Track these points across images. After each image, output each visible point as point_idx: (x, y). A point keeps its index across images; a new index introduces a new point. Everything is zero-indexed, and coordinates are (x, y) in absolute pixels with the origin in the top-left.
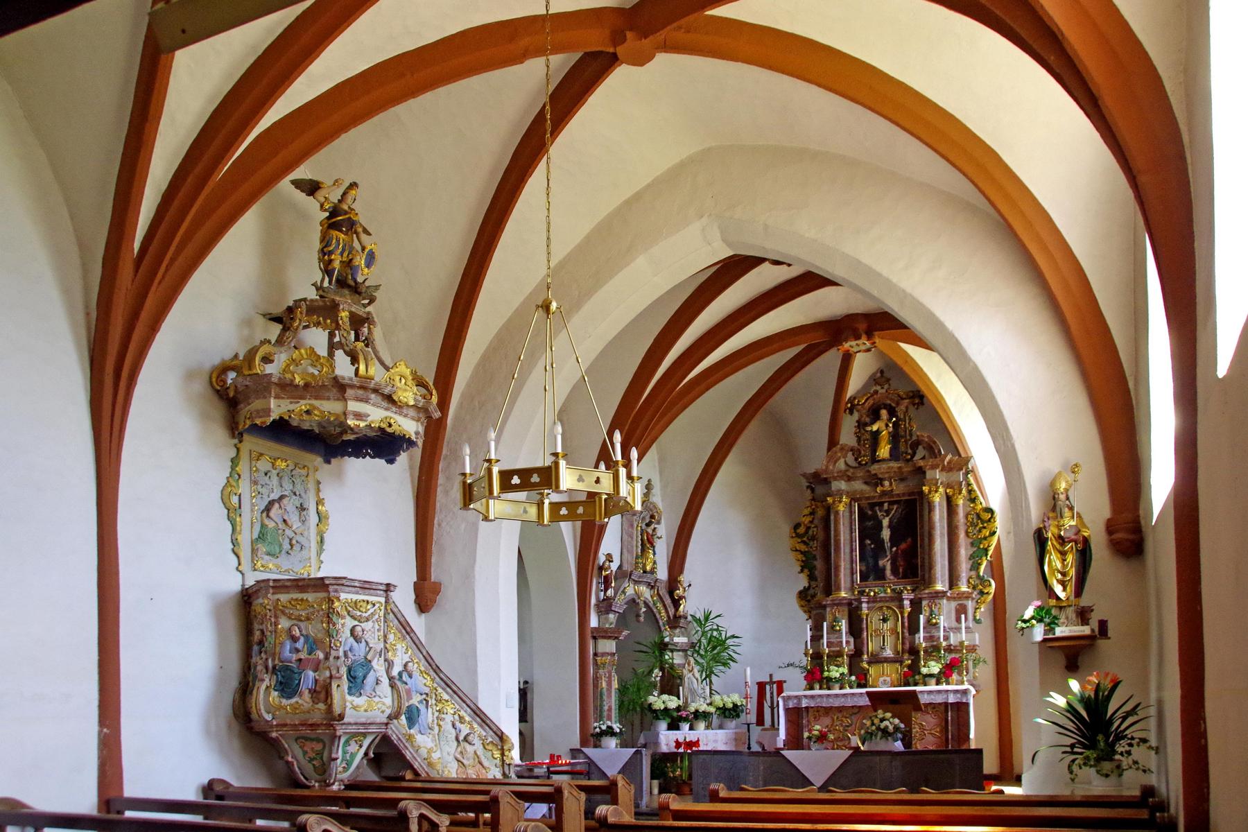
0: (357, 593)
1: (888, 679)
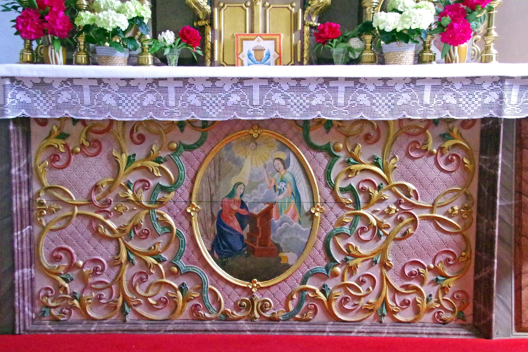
1: (269, 46)
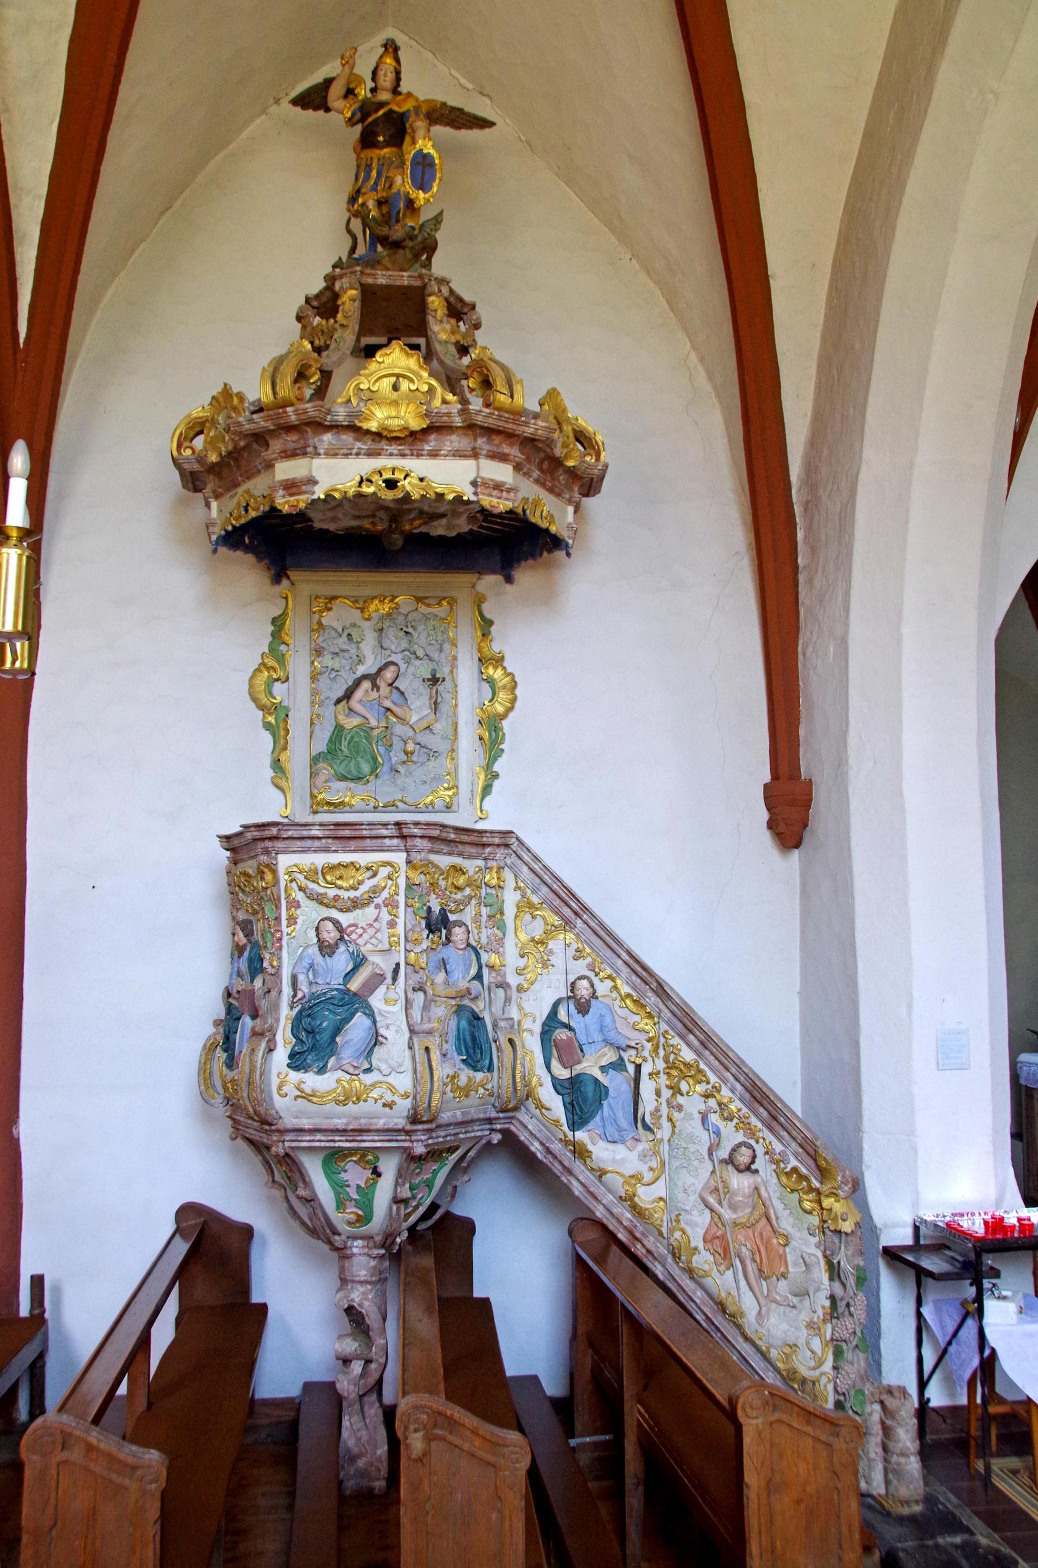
0: (326, 850)
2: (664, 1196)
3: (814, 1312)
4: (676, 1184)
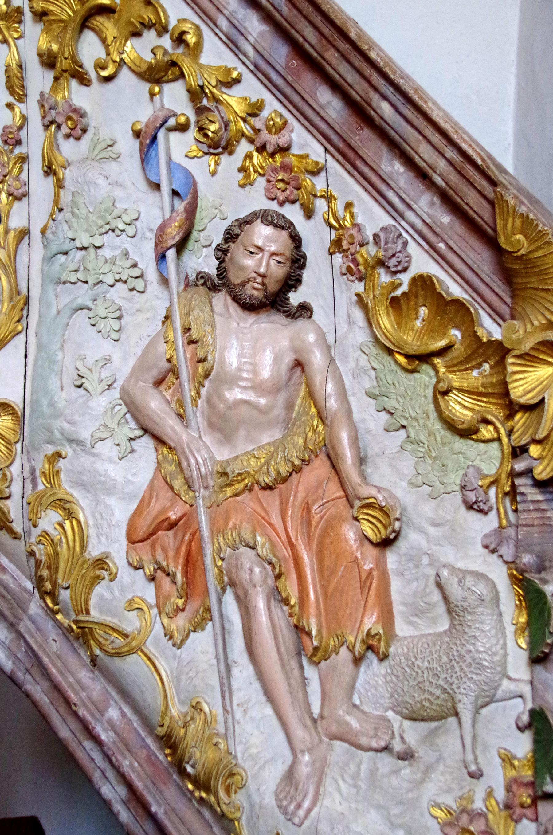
2: (16, 399)
3: (476, 775)
4: (52, 361)
